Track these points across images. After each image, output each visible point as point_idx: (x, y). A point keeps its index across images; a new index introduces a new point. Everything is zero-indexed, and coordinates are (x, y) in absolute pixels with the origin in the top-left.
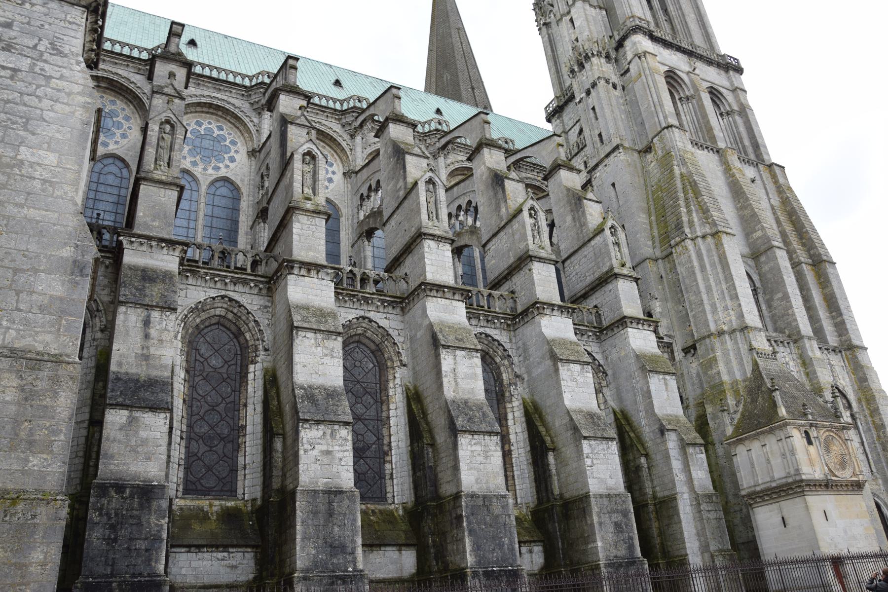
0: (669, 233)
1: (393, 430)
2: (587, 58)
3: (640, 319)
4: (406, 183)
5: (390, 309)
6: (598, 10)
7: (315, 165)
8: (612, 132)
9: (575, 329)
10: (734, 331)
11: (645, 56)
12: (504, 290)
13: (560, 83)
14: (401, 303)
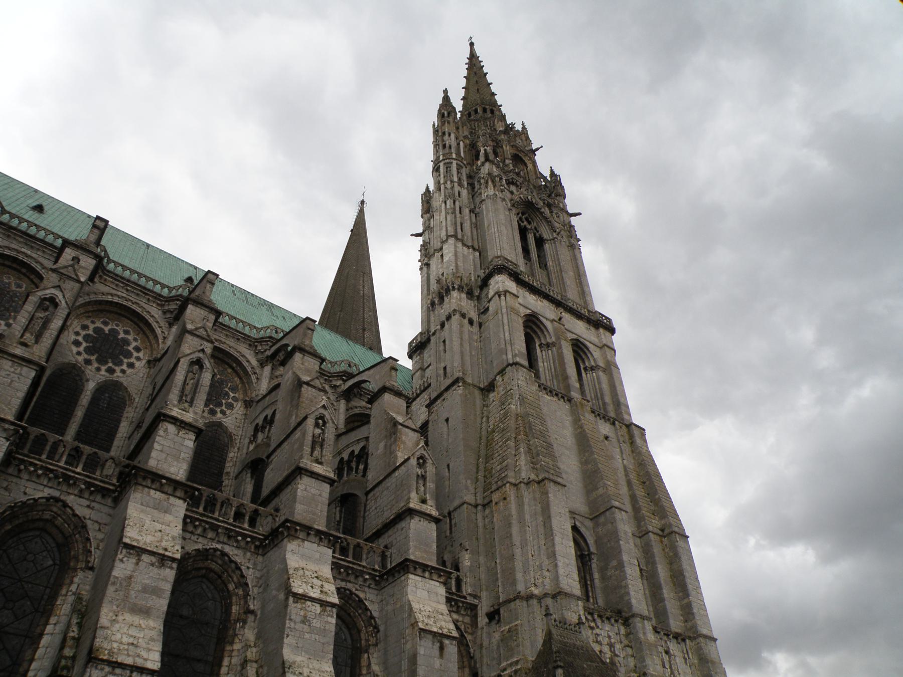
2: (448, 291)
5: (99, 498)
6: (471, 250)
9: (333, 563)
10: (546, 595)
11: (505, 296)
12: (270, 508)
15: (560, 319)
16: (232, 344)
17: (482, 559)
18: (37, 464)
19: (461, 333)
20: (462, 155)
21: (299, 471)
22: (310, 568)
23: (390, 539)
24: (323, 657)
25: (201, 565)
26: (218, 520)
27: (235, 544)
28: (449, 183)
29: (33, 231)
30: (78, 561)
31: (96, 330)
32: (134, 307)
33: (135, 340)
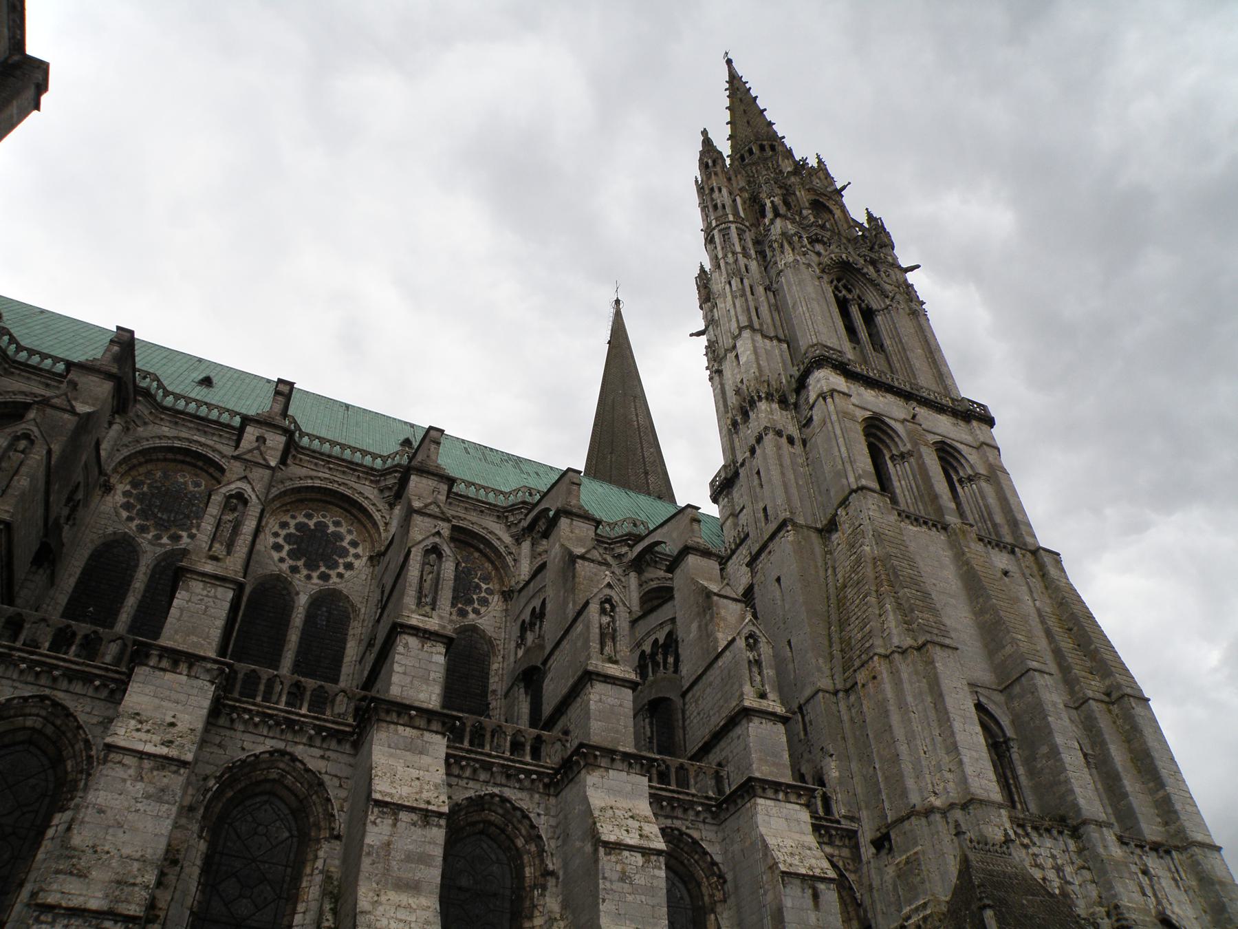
2: (752, 403)
5: (334, 744)
6: (775, 342)
8: (779, 502)
9: (651, 795)
10: (952, 806)
11: (832, 397)
12: (556, 732)
14: (352, 734)
15: (914, 417)
16: (474, 519)
17: (854, 766)
18: (251, 711)
19: (780, 457)
20: (742, 214)
21: (588, 677)
22: (620, 805)
23: (724, 754)
25: (476, 818)
26: (489, 755)
27: (517, 785)
28: (730, 255)
29: (203, 411)
30: (319, 829)
31: (300, 527)
32: (341, 489)
33: (350, 532)
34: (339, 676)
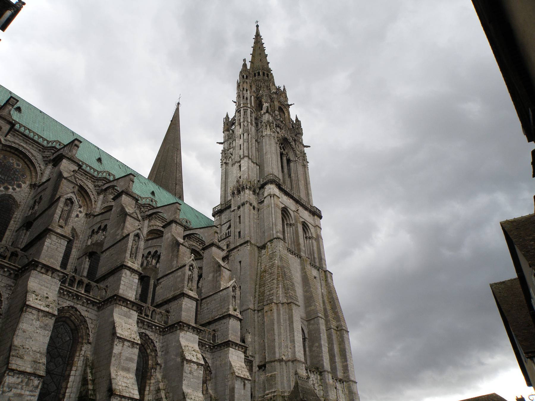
0: (263, 302)
1: (70, 384)
2: (243, 189)
3: (237, 344)
4: (122, 233)
5: (91, 306)
7: (71, 207)
8: (246, 232)
9: (199, 342)
10: (289, 361)
12: (162, 310)
13: (225, 197)
14: (99, 303)
15: (297, 210)
17: (256, 338)
19: (250, 214)
23: (217, 327)
24: (198, 390)
26: (144, 318)
28: (246, 122)
29: (27, 132)
34: (67, 262)
